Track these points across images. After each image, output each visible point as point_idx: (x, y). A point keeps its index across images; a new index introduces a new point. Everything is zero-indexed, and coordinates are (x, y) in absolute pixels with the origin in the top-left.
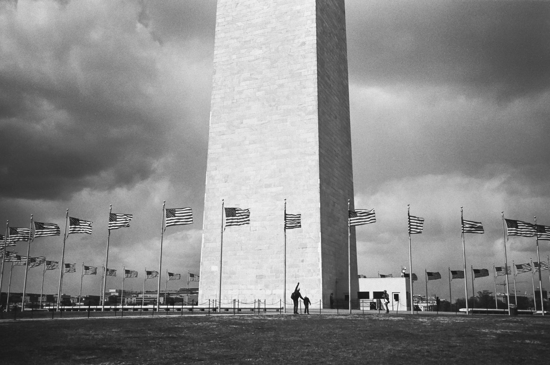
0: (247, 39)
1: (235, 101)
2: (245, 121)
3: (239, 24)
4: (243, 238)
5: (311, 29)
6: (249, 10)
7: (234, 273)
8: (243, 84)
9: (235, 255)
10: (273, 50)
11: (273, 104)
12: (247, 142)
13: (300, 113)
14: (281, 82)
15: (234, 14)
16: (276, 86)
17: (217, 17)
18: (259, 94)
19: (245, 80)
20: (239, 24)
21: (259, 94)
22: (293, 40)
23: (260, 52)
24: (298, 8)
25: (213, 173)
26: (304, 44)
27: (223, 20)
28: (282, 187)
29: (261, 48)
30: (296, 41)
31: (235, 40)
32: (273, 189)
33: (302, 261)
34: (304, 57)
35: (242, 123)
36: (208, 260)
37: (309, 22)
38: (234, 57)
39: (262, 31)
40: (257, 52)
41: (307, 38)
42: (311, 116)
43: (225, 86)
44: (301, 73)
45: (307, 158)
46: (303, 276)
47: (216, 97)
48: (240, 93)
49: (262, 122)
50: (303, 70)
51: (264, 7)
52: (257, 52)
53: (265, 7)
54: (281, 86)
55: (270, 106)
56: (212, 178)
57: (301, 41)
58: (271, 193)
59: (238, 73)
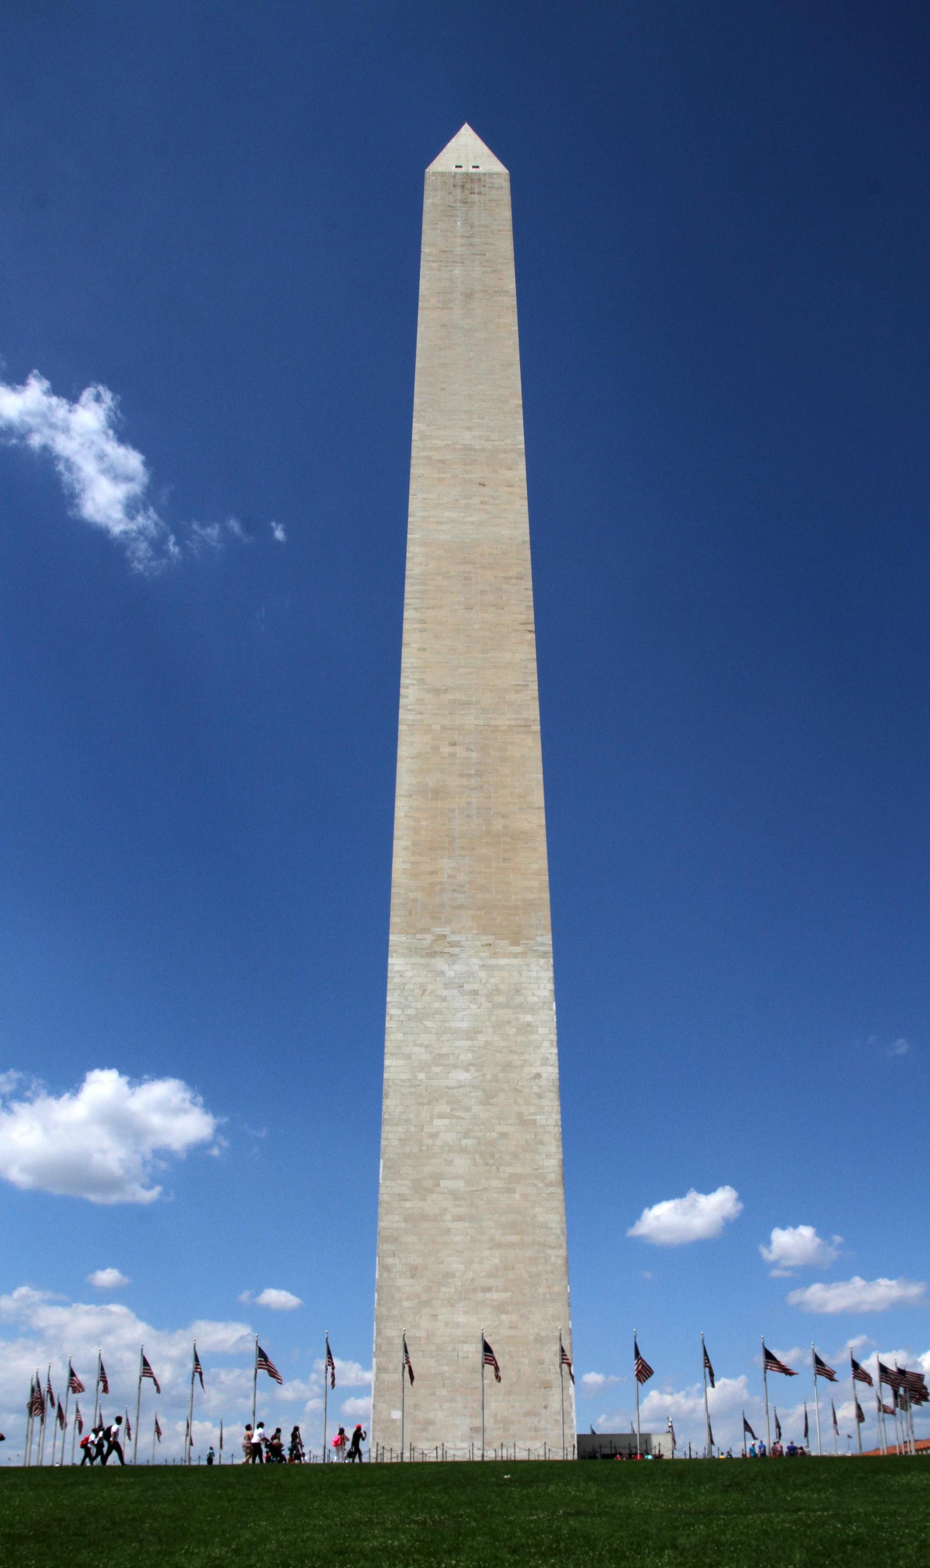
0: (443, 1051)
1: (424, 1148)
2: (443, 1183)
3: (429, 1024)
4: (446, 1368)
5: (549, 1056)
6: (444, 1004)
7: (431, 1423)
8: (438, 1122)
9: (433, 1394)
10: (489, 1077)
11: (491, 1161)
12: (448, 1217)
13: (535, 1181)
14: (504, 1129)
15: (419, 1005)
16: (494, 1135)
17: (389, 1005)
18: (464, 1142)
19: (441, 1116)
20: (429, 1024)
21: (464, 1142)
22: (522, 1067)
24: (529, 1018)
25: (389, 1261)
26: (538, 1076)
27: (399, 1012)
28: (508, 1294)
29: (468, 1071)
30: (526, 1070)
31: (423, 1050)
32: (495, 1296)
33: (546, 1407)
34: (540, 1096)
35: (438, 1185)
36: (385, 1402)
38: (421, 1076)
40: (462, 1076)
42: (552, 1190)
43: (406, 1120)
44: (535, 1120)
45: (549, 1252)
46: (546, 1429)
47: (389, 1136)
48: (434, 1136)
49: (474, 1189)
50: (538, 1117)
51: (471, 1006)
52: (462, 1076)
53: (473, 1006)
54: (504, 1135)
55: (487, 1164)
56: (386, 1268)
57: (534, 1070)
58: (492, 1301)
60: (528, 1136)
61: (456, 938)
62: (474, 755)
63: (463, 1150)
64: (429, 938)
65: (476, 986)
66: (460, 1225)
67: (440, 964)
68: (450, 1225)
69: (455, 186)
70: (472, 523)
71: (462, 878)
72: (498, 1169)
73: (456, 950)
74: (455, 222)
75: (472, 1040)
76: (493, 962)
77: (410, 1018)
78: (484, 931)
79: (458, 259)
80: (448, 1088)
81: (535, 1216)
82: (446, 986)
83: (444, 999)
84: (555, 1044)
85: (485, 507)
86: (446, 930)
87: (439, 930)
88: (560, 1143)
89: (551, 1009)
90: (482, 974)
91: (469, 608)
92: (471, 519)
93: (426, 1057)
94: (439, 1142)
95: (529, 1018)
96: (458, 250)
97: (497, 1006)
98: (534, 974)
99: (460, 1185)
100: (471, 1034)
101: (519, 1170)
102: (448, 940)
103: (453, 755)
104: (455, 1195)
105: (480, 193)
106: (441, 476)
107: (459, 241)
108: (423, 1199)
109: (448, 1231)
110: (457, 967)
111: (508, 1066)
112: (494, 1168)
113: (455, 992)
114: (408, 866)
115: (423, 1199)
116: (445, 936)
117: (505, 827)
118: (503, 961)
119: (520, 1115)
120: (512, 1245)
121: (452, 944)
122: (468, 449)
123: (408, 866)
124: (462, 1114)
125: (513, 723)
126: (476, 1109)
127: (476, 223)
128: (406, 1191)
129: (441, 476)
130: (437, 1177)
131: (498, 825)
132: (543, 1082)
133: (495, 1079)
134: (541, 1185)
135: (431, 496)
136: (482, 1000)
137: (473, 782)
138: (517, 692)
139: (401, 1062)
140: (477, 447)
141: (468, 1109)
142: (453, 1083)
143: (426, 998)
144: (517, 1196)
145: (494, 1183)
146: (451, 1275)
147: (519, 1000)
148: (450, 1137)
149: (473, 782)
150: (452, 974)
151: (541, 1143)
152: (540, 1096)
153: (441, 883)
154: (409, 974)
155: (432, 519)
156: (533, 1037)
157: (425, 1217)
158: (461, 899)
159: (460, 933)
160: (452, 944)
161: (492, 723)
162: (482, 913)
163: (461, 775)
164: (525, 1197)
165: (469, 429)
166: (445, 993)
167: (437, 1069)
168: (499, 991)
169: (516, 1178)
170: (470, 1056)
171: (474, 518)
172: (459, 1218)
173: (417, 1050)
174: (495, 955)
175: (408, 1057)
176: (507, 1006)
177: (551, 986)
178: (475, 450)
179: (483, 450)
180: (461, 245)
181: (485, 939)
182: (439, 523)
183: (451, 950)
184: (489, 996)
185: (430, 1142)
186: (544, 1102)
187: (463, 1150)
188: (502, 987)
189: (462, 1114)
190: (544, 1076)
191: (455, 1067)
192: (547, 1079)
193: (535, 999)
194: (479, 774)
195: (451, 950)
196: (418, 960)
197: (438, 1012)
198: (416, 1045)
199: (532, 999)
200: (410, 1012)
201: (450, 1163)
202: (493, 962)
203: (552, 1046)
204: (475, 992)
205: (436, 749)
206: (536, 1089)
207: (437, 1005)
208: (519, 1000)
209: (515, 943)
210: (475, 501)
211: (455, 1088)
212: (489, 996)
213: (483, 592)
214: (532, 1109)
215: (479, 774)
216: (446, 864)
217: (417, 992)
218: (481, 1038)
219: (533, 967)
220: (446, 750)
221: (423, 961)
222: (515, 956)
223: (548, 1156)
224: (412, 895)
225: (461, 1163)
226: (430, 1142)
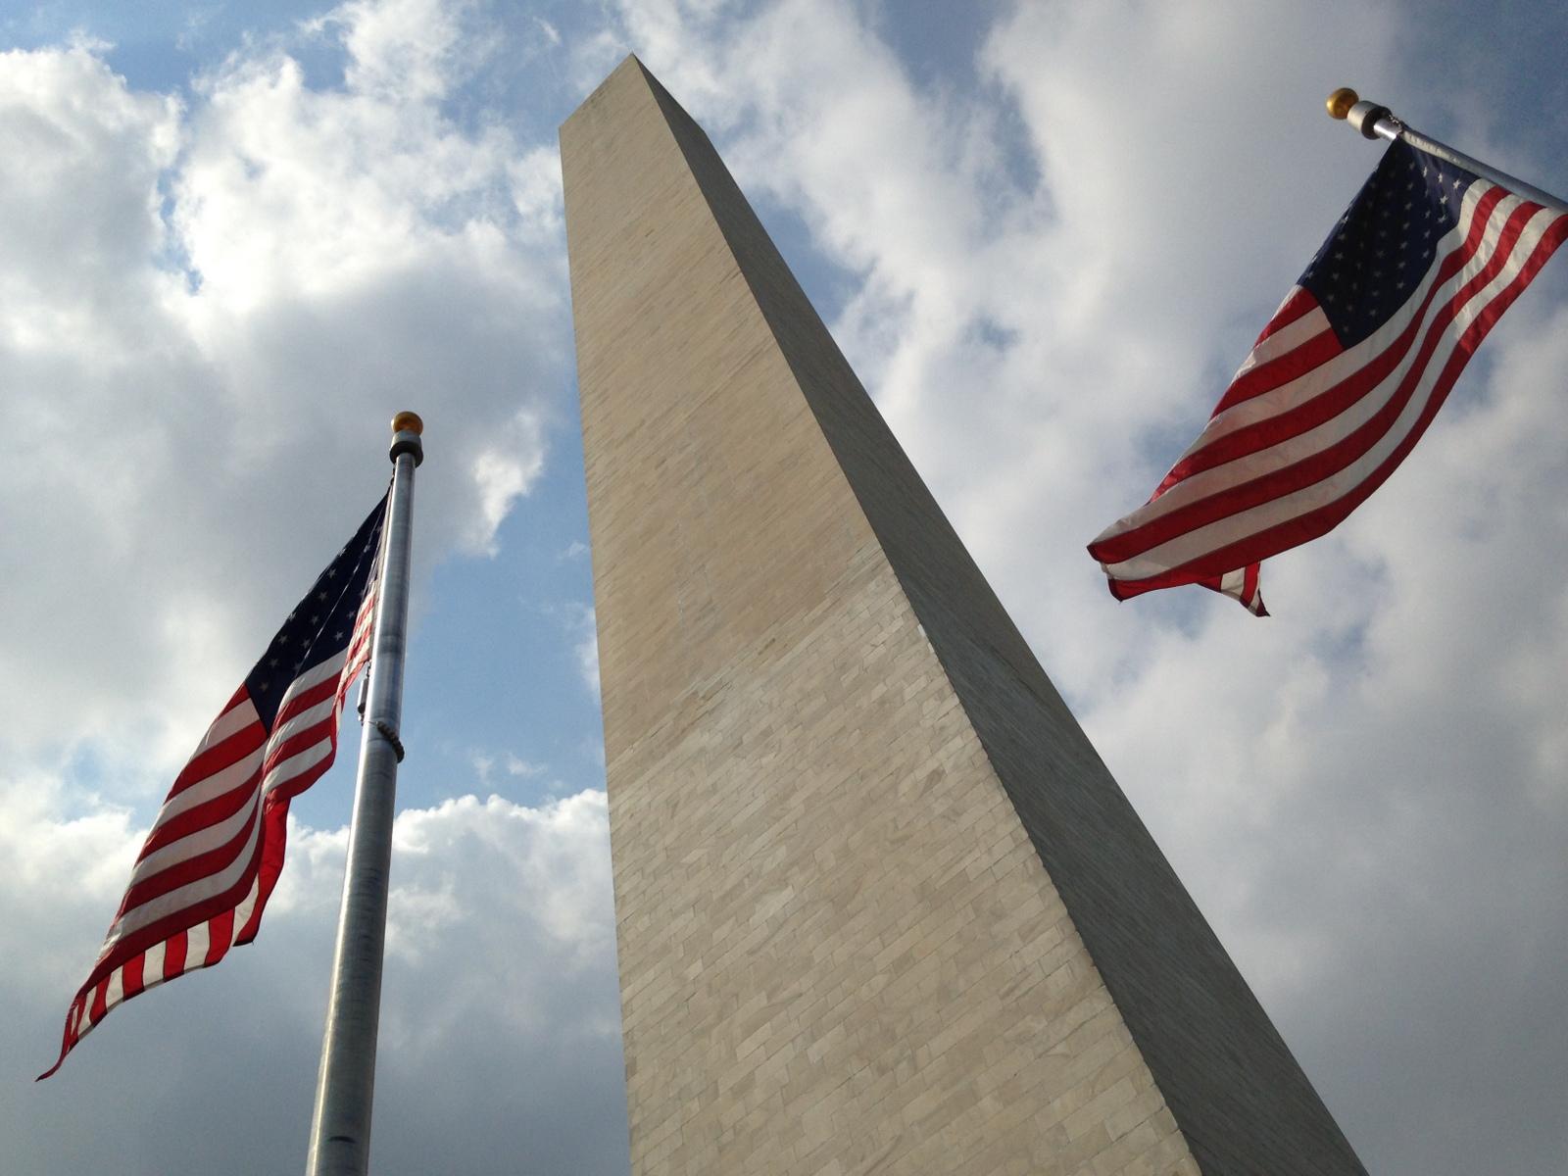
0: (728, 886)
3: (691, 857)
6: (714, 800)
8: (747, 1048)
15: (669, 840)
16: (880, 980)
19: (750, 1029)
20: (691, 857)
21: (815, 1052)
23: (787, 894)
24: (879, 690)
26: (937, 775)
29: (782, 882)
30: (905, 787)
37: (932, 703)
38: (696, 969)
39: (777, 827)
40: (776, 903)
41: (942, 754)
42: (1073, 1017)
48: (742, 1090)
50: (968, 861)
52: (776, 903)
54: (903, 963)
55: (882, 1071)
57: (921, 774)
59: (720, 1018)
67: (695, 741)
72: (913, 1059)
73: (718, 698)
75: (778, 819)
80: (752, 952)
81: (1060, 1128)
83: (714, 789)
84: (948, 690)
88: (1045, 879)
89: (918, 640)
94: (758, 1095)
98: (865, 615)
102: (701, 695)
112: (904, 1065)
116: (695, 693)
132: (951, 780)
134: (1038, 1025)
139: (650, 974)
144: (987, 1103)
151: (998, 915)
170: (782, 852)
177: (905, 605)
183: (709, 705)
190: (948, 766)
192: (956, 767)
193: (882, 650)
195: (709, 705)
198: (675, 916)
203: (942, 698)
204: (766, 733)
206: (939, 808)
211: (766, 941)
222: (818, 621)
223: (1028, 933)
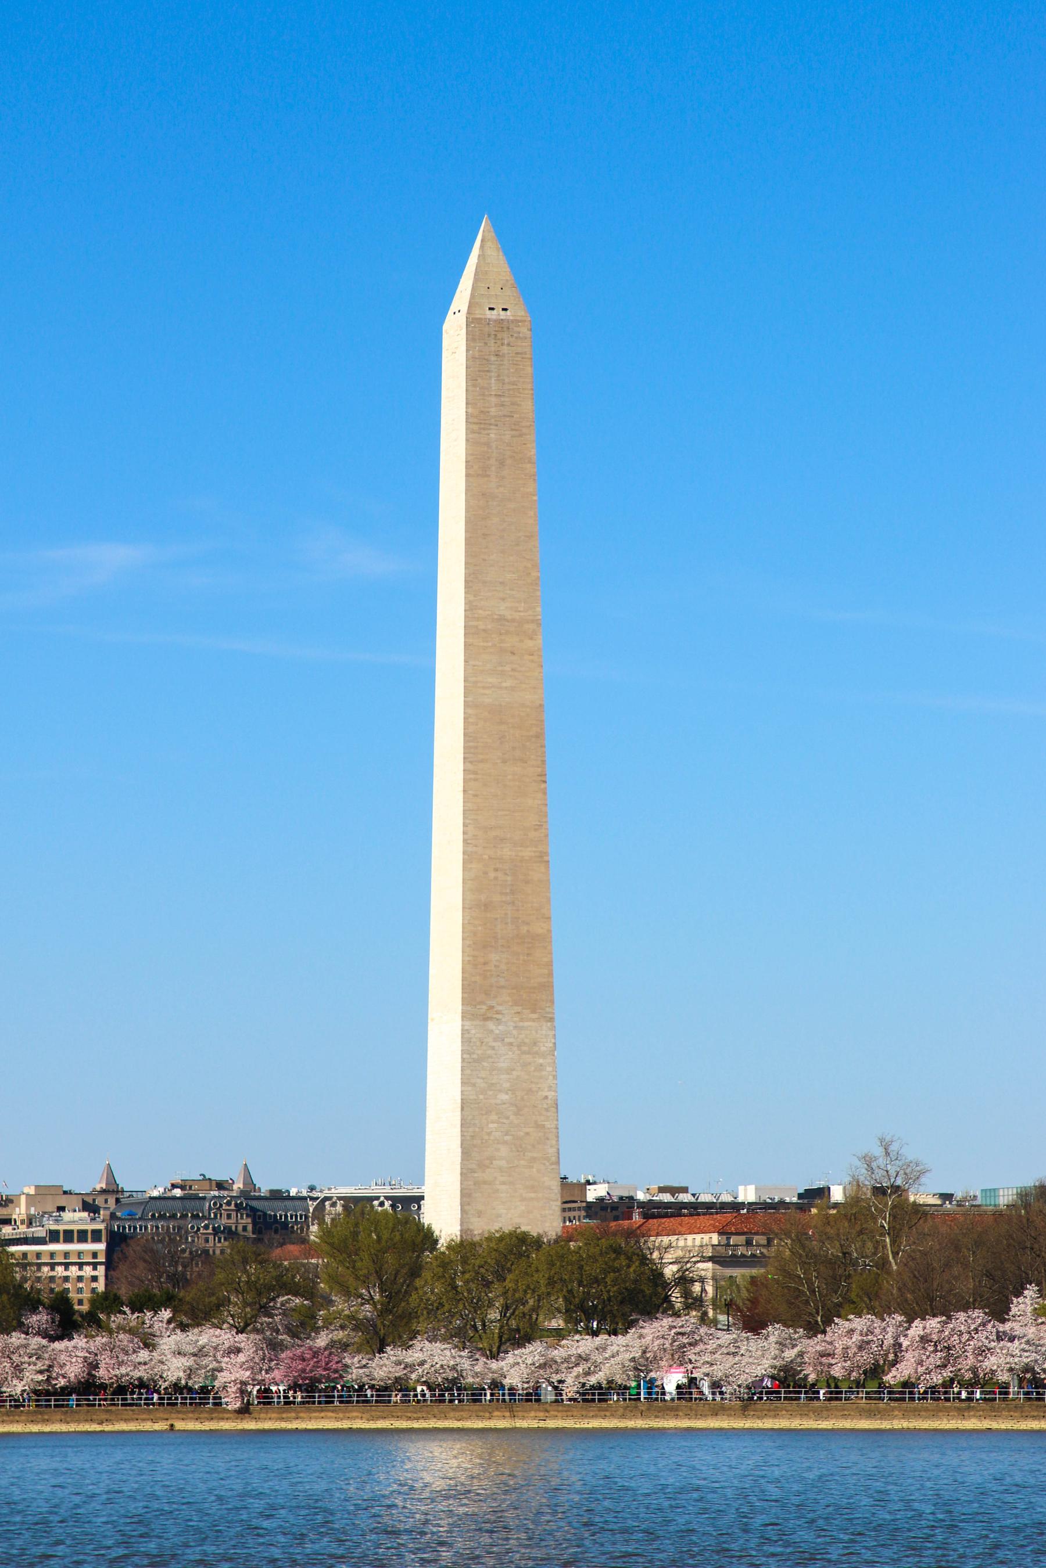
3: (485, 1064)
8: (491, 1125)
14: (527, 1130)
15: (480, 1052)
16: (522, 1134)
18: (507, 1138)
19: (493, 1122)
20: (485, 1064)
23: (507, 1097)
24: (541, 1061)
26: (546, 1097)
30: (540, 1093)
38: (481, 1097)
40: (504, 1097)
48: (489, 1134)
52: (504, 1097)
54: (527, 1134)
60: (540, 1134)
61: (500, 1008)
62: (509, 878)
63: (505, 1143)
64: (484, 1007)
65: (512, 1040)
66: (503, 1187)
67: (491, 1025)
68: (499, 1187)
69: (489, 335)
70: (506, 688)
71: (503, 967)
74: (490, 377)
76: (521, 1024)
77: (475, 1061)
78: (516, 1003)
79: (493, 421)
82: (495, 1040)
83: (493, 1048)
85: (516, 674)
86: (493, 1003)
87: (489, 1003)
90: (515, 1032)
91: (504, 762)
92: (504, 685)
93: (483, 1085)
95: (541, 1061)
96: (493, 411)
97: (524, 1053)
98: (544, 1032)
99: (503, 1163)
100: (509, 1071)
101: (535, 1155)
103: (496, 878)
104: (501, 1169)
105: (508, 345)
106: (485, 644)
107: (494, 400)
108: (484, 1172)
109: (497, 1191)
110: (500, 1027)
111: (530, 1091)
113: (499, 1044)
114: (470, 958)
115: (484, 1172)
117: (528, 931)
118: (526, 1024)
119: (536, 1122)
120: (532, 1199)
121: (498, 1013)
122: (502, 619)
123: (470, 958)
124: (505, 1121)
125: (533, 854)
126: (512, 1117)
127: (507, 380)
128: (474, 1166)
129: (485, 644)
130: (491, 1159)
131: (524, 929)
133: (522, 1099)
135: (477, 663)
136: (515, 1048)
137: (508, 898)
138: (536, 830)
140: (509, 617)
141: (508, 1118)
142: (499, 1102)
143: (484, 1048)
145: (522, 1162)
146: (499, 1216)
147: (536, 1049)
148: (498, 1134)
149: (508, 898)
150: (497, 1032)
152: (547, 1110)
153: (490, 971)
154: (473, 1032)
155: (479, 685)
156: (544, 1073)
157: (485, 1183)
158: (502, 982)
159: (501, 1005)
160: (498, 1013)
161: (520, 854)
162: (514, 991)
163: (501, 893)
164: (539, 1171)
165: (503, 599)
166: (494, 1044)
167: (491, 1093)
168: (525, 1043)
169: (534, 1159)
171: (508, 683)
172: (504, 1183)
173: (479, 1081)
174: (522, 1020)
175: (474, 1085)
176: (529, 1053)
178: (508, 621)
179: (513, 620)
180: (496, 405)
181: (519, 1009)
182: (484, 688)
183: (497, 1016)
184: (519, 1046)
185: (486, 1137)
186: (549, 1114)
187: (505, 1143)
188: (527, 1041)
189: (505, 1121)
191: (500, 1091)
194: (512, 892)
195: (497, 1016)
196: (477, 1022)
197: (490, 1057)
199: (543, 1049)
200: (475, 1056)
201: (498, 1150)
202: (521, 1024)
204: (511, 1044)
205: (486, 873)
206: (545, 1106)
207: (489, 1052)
208: (536, 1049)
209: (534, 1012)
210: (508, 668)
212: (519, 1046)
213: (514, 748)
214: (543, 1118)
215: (512, 892)
216: (494, 957)
217: (478, 1043)
218: (515, 1073)
219: (544, 1027)
220: (492, 875)
221: (481, 1023)
222: (533, 1020)
224: (473, 979)
225: (504, 1151)
226: (486, 1137)
